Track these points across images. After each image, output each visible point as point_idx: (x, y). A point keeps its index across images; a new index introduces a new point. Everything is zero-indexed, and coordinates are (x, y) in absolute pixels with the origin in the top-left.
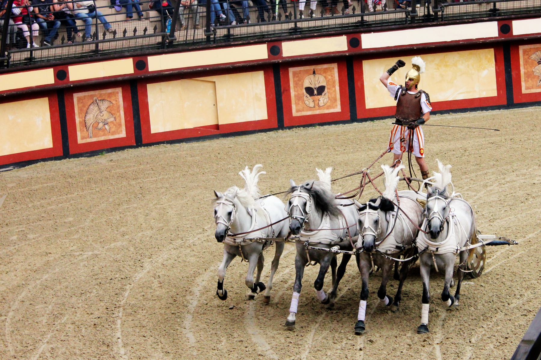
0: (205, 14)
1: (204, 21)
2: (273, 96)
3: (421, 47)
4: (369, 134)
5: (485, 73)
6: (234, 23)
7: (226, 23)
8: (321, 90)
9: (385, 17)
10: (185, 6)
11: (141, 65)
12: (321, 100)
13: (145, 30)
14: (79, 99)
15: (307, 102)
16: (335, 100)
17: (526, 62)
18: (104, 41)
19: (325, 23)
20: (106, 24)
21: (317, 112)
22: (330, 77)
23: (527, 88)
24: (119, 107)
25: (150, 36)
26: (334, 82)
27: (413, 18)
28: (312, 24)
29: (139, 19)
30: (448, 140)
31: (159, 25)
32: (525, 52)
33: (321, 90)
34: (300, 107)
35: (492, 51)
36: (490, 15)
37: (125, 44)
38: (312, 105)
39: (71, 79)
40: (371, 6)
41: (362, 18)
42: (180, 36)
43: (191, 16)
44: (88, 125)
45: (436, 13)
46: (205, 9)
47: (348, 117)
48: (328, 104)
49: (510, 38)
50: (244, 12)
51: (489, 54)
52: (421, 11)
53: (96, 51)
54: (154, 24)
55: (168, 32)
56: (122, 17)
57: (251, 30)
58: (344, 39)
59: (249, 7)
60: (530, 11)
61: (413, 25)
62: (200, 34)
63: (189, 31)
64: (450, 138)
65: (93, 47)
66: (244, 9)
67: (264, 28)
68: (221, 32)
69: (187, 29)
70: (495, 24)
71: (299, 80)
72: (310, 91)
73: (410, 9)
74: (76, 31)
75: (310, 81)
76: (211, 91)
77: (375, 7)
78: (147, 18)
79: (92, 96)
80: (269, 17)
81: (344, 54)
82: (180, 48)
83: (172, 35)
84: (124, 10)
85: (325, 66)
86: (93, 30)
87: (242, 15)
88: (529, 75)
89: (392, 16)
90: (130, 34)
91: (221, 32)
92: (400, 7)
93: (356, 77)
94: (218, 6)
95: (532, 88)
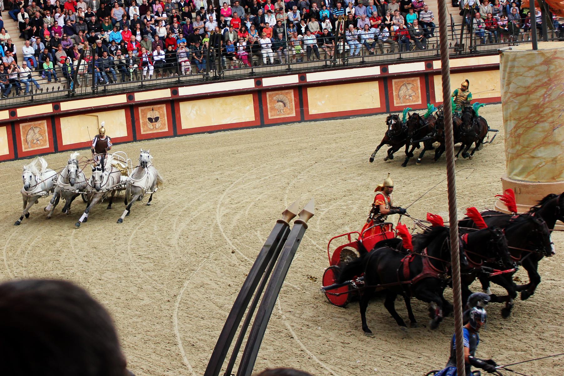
0: (91, 78)
1: (91, 82)
2: (130, 123)
3: (212, 94)
4: (184, 143)
5: (248, 108)
6: (108, 83)
7: (104, 83)
8: (157, 119)
9: (192, 78)
10: (80, 75)
11: (56, 107)
12: (157, 124)
13: (59, 88)
14: (23, 127)
15: (149, 126)
16: (165, 124)
17: (271, 101)
18: (36, 95)
19: (158, 82)
20: (37, 85)
21: (155, 132)
22: (161, 112)
23: (271, 116)
24: (45, 131)
25: (61, 91)
26: (164, 115)
27: (207, 78)
28: (151, 83)
29: (55, 82)
30: (228, 146)
31: (66, 85)
32: (270, 96)
33: (157, 119)
34: (145, 129)
35: (251, 95)
36: (250, 76)
37: (48, 96)
38: (152, 127)
39: (18, 116)
40: (183, 72)
41: (179, 79)
42: (78, 91)
43: (84, 79)
44: (28, 141)
45: (220, 75)
46: (91, 76)
47: (172, 134)
48: (161, 127)
49: (261, 88)
50: (113, 77)
51: (250, 97)
52: (211, 74)
53: (32, 100)
54: (63, 85)
55: (71, 89)
56: (46, 81)
57: (117, 87)
58: (169, 91)
59: (117, 74)
60: (272, 73)
61: (207, 82)
62: (89, 90)
63: (83, 88)
64: (229, 144)
65: (30, 98)
66: (113, 75)
67: (124, 86)
68: (101, 88)
69: (81, 87)
70: (253, 80)
71: (145, 114)
72: (150, 120)
73: (205, 73)
74: (21, 89)
75: (151, 114)
76: (96, 121)
77: (186, 73)
78: (60, 82)
79: (30, 125)
80: (127, 79)
81: (169, 99)
82: (78, 97)
83: (73, 90)
84: (47, 77)
85: (159, 106)
86: (30, 88)
87: (113, 80)
88: (273, 109)
89: (195, 77)
90: (50, 90)
91: (101, 88)
92: (200, 72)
93: (176, 112)
94: (99, 74)
95: (275, 116)
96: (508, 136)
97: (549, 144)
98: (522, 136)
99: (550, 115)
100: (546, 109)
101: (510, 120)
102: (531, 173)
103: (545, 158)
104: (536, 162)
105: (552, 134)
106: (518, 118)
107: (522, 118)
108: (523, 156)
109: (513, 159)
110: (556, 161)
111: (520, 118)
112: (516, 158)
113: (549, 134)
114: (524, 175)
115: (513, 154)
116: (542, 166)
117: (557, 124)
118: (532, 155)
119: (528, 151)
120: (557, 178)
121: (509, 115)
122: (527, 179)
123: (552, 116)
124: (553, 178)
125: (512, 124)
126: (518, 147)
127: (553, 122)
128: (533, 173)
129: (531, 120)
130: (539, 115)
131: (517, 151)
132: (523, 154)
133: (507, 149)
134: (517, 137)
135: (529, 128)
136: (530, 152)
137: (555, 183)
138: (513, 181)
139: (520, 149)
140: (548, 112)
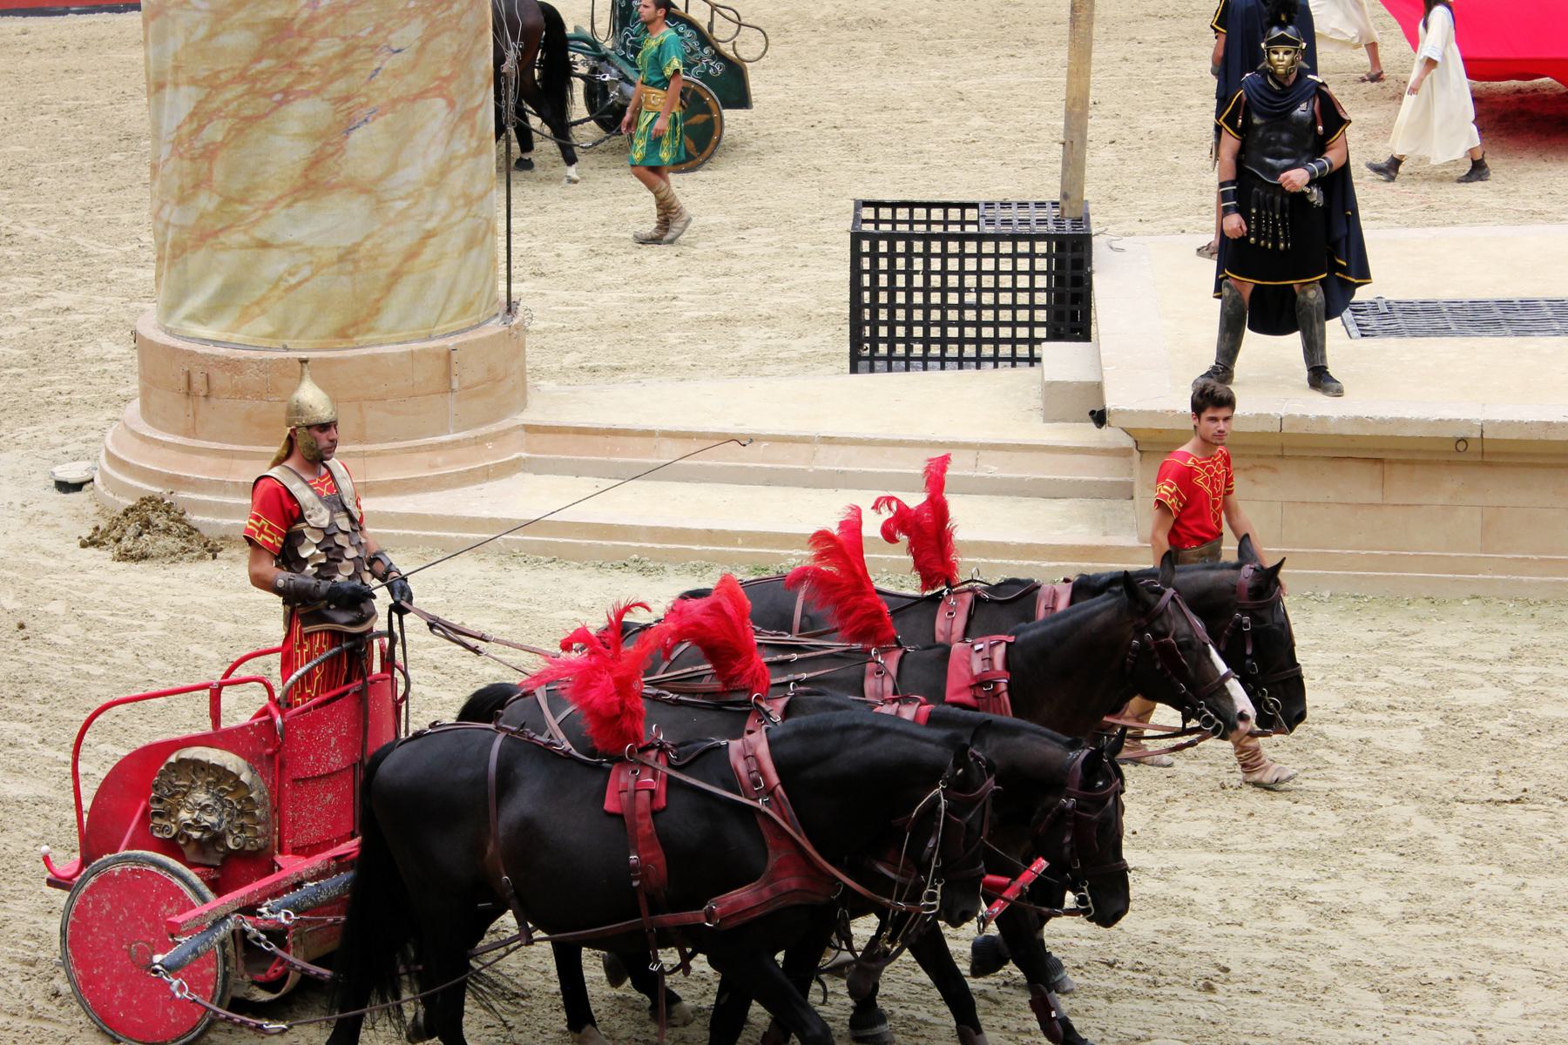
96: (165, 151)
97: (330, 188)
98: (223, 154)
99: (336, 66)
100: (322, 43)
101: (177, 85)
102: (257, 310)
103: (310, 251)
104: (275, 265)
105: (340, 149)
106: (205, 79)
107: (224, 77)
108: (222, 238)
109: (184, 251)
110: (356, 262)
111: (217, 74)
112: (196, 248)
113: (330, 149)
114: (227, 320)
115: (182, 228)
116: (299, 284)
117: (362, 105)
118: (260, 233)
119: (242, 217)
120: (357, 333)
121: (170, 63)
122: (236, 337)
123: (346, 71)
124: (343, 334)
125: (182, 101)
126: (206, 202)
127: (347, 99)
128: (264, 312)
129: (259, 85)
130: (291, 65)
131: (202, 216)
132: (221, 230)
133: (161, 208)
134: (202, 156)
135: (247, 119)
136: (255, 223)
137: (349, 353)
138: (180, 344)
139: (211, 206)
140: (330, 52)
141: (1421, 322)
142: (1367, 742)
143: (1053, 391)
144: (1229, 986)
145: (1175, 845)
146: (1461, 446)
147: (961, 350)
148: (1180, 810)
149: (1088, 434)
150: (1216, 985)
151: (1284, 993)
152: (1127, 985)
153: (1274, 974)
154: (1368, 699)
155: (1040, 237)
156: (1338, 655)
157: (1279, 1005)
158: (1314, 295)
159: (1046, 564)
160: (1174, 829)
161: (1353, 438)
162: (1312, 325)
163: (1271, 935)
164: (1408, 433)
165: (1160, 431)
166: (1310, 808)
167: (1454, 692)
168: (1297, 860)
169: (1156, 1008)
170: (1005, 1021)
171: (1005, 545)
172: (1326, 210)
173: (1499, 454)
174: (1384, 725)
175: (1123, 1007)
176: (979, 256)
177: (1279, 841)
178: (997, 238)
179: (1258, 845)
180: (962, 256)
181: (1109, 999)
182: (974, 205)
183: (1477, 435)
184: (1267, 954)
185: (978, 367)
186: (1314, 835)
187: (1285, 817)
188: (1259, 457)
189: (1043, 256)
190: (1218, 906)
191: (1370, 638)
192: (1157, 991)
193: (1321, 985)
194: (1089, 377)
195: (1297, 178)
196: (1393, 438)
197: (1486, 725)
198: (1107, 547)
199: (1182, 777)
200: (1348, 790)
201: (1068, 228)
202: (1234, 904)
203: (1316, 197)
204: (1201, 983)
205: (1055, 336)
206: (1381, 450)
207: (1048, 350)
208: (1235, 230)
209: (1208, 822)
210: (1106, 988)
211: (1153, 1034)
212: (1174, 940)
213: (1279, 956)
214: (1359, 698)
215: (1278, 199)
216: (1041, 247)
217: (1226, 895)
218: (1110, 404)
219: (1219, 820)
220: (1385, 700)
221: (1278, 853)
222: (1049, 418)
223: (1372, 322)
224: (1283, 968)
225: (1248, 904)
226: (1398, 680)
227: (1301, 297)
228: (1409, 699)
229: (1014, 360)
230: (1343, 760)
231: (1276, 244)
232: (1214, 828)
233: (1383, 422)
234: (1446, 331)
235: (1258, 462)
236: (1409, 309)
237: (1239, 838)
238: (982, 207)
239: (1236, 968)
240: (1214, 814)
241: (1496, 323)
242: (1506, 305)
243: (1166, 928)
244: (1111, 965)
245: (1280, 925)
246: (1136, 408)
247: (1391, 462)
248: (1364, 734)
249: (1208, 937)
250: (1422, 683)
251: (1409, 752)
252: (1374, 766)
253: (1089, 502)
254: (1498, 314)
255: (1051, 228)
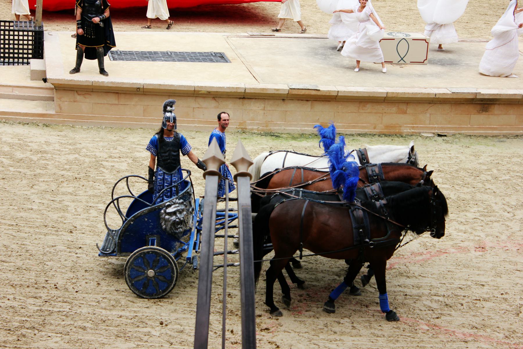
141: (128, 57)
142: (114, 166)
143: (33, 72)
144: (76, 232)
145: (63, 194)
146: (138, 90)
147: (9, 60)
148: (65, 184)
149: (41, 84)
150: (73, 231)
151: (91, 233)
152: (50, 232)
153: (88, 228)
154: (114, 155)
155: (30, 31)
156: (106, 143)
157: (89, 236)
158: (101, 50)
159: (31, 118)
160: (63, 190)
161: (111, 87)
162: (100, 58)
163: (88, 218)
164: (125, 86)
165: (61, 84)
166: (98, 184)
167: (136, 153)
168: (95, 198)
169: (58, 238)
170: (17, 242)
171: (20, 113)
172: (104, 28)
173: (148, 92)
174: (118, 162)
175: (49, 237)
176: (14, 35)
177: (90, 193)
178: (18, 31)
179: (85, 194)
180: (9, 35)
181: (45, 235)
182: (13, 22)
183: (142, 87)
184: (86, 223)
185: (13, 65)
186: (99, 191)
187: (92, 186)
188: (87, 91)
189: (31, 36)
190: (74, 210)
191: (115, 139)
192: (58, 233)
193: (100, 231)
194: (44, 69)
195: (97, 20)
196: (121, 87)
197: (144, 162)
198: (47, 114)
199: (65, 176)
200: (108, 179)
201: (37, 29)
202: (78, 210)
203: (102, 24)
204: (69, 231)
205: (34, 57)
206: (118, 90)
207: (31, 61)
208: (81, 33)
209: (72, 188)
210: (44, 233)
211: (57, 245)
212: (62, 219)
213: (90, 223)
214: (112, 155)
215: (92, 25)
216: (30, 34)
217: (76, 207)
218: (48, 77)
219: (75, 187)
220: (118, 155)
221: (90, 196)
222: (32, 79)
223: (116, 56)
224: (90, 227)
225: (82, 210)
226: (121, 150)
227: (98, 50)
228: (124, 155)
229: (23, 63)
230: (107, 171)
231: (91, 37)
232: (73, 189)
233: (118, 83)
234: (134, 59)
235: (86, 93)
236: (125, 53)
237: (80, 192)
238: (14, 22)
239: (79, 227)
240: (74, 185)
241: (148, 57)
242: (150, 53)
243: (60, 216)
244: (46, 226)
245: (90, 215)
246: (54, 78)
247: (120, 93)
248: (113, 164)
249: (71, 218)
250: (128, 151)
251: (124, 169)
252: (115, 173)
253: (42, 102)
254: (148, 55)
255: (33, 29)
